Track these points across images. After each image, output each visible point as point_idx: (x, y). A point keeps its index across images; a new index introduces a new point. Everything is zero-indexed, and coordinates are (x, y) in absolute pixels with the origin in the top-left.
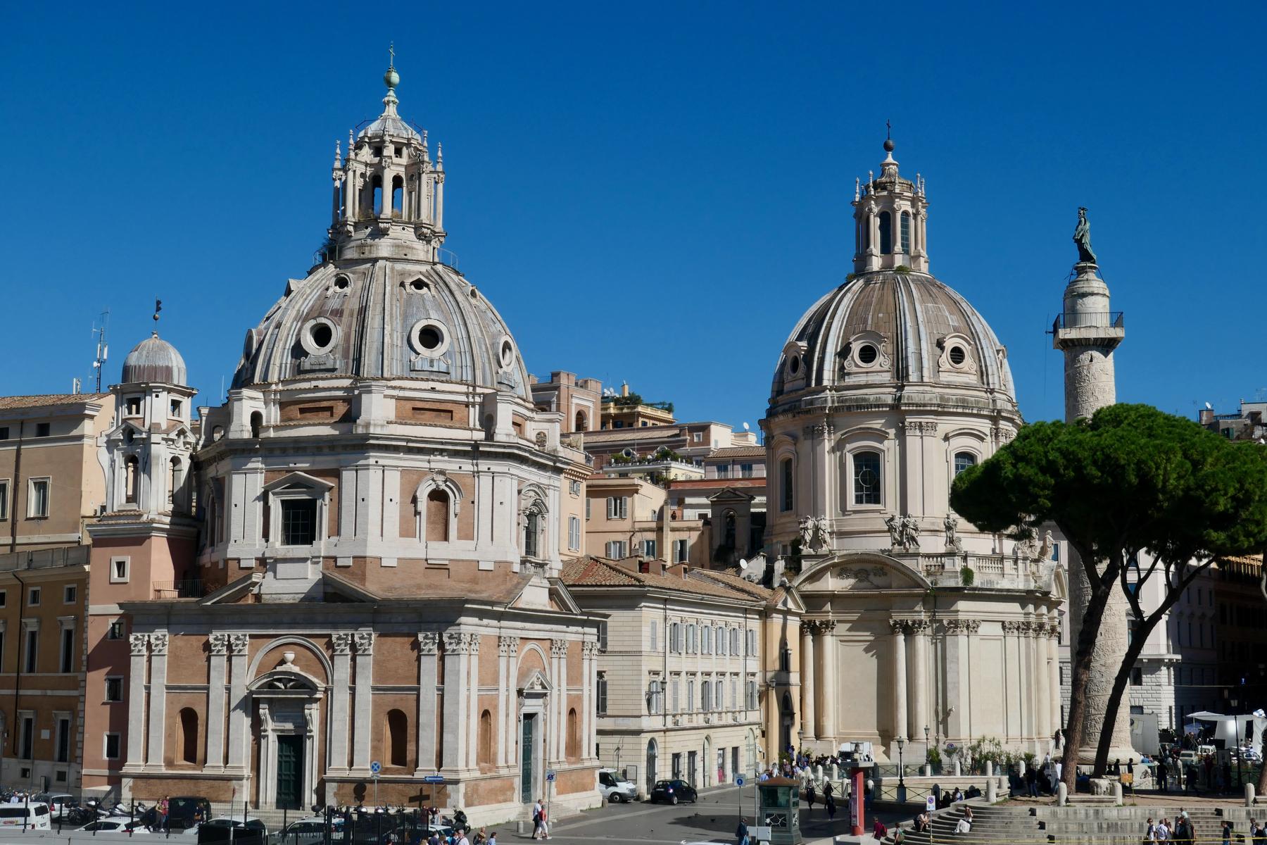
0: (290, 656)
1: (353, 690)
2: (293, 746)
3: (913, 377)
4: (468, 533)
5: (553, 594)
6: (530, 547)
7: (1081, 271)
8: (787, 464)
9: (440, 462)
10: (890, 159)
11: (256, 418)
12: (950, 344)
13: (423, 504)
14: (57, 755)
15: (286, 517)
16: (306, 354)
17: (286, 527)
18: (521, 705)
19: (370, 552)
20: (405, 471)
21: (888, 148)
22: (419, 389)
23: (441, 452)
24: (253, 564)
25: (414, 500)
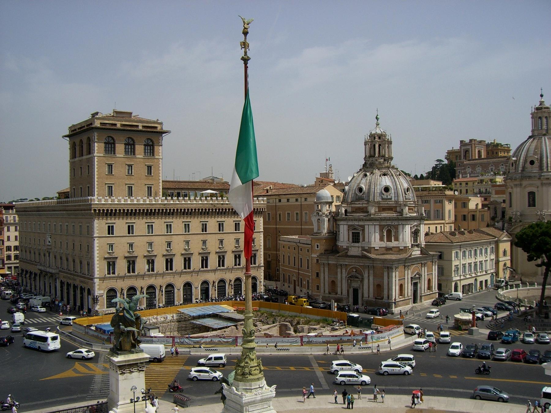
1: (369, 280)
2: (356, 291)
3: (545, 170)
4: (397, 239)
5: (421, 251)
6: (415, 240)
8: (510, 193)
9: (389, 223)
11: (346, 211)
13: (385, 234)
15: (353, 236)
16: (357, 195)
17: (353, 239)
18: (412, 281)
19: (372, 246)
20: (380, 225)
22: (384, 204)
23: (389, 220)
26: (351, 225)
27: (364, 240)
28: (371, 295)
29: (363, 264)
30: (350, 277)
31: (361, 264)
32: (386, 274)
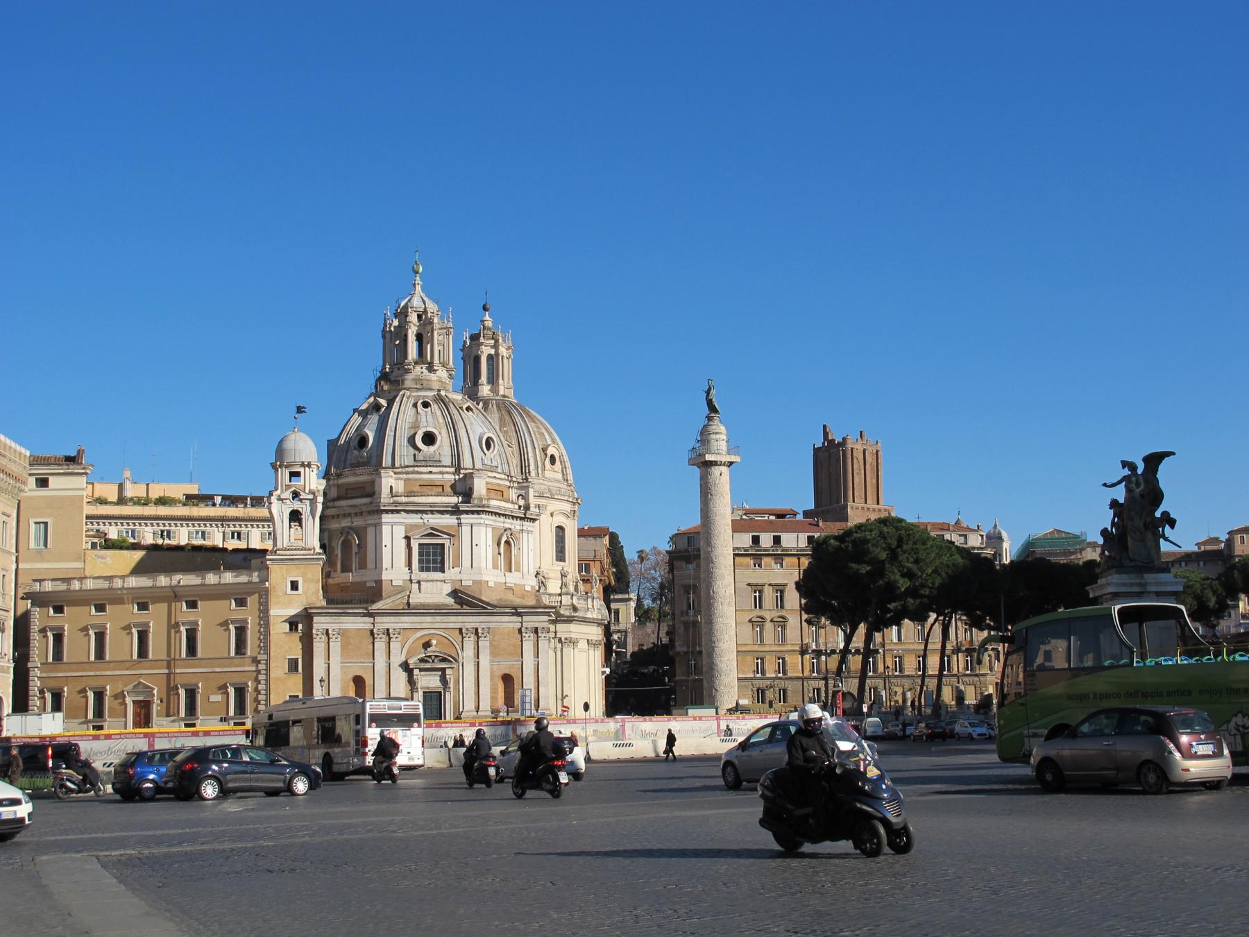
0: (434, 642)
7: (709, 418)
9: (509, 523)
10: (487, 317)
12: (551, 451)
14: (231, 713)
15: (420, 554)
16: (419, 450)
17: (420, 561)
19: (485, 578)
20: (494, 529)
21: (485, 309)
24: (400, 583)
25: (499, 544)
26: (416, 526)
27: (457, 563)
28: (485, 705)
29: (459, 626)
30: (422, 660)
31: (451, 626)
32: (528, 646)
